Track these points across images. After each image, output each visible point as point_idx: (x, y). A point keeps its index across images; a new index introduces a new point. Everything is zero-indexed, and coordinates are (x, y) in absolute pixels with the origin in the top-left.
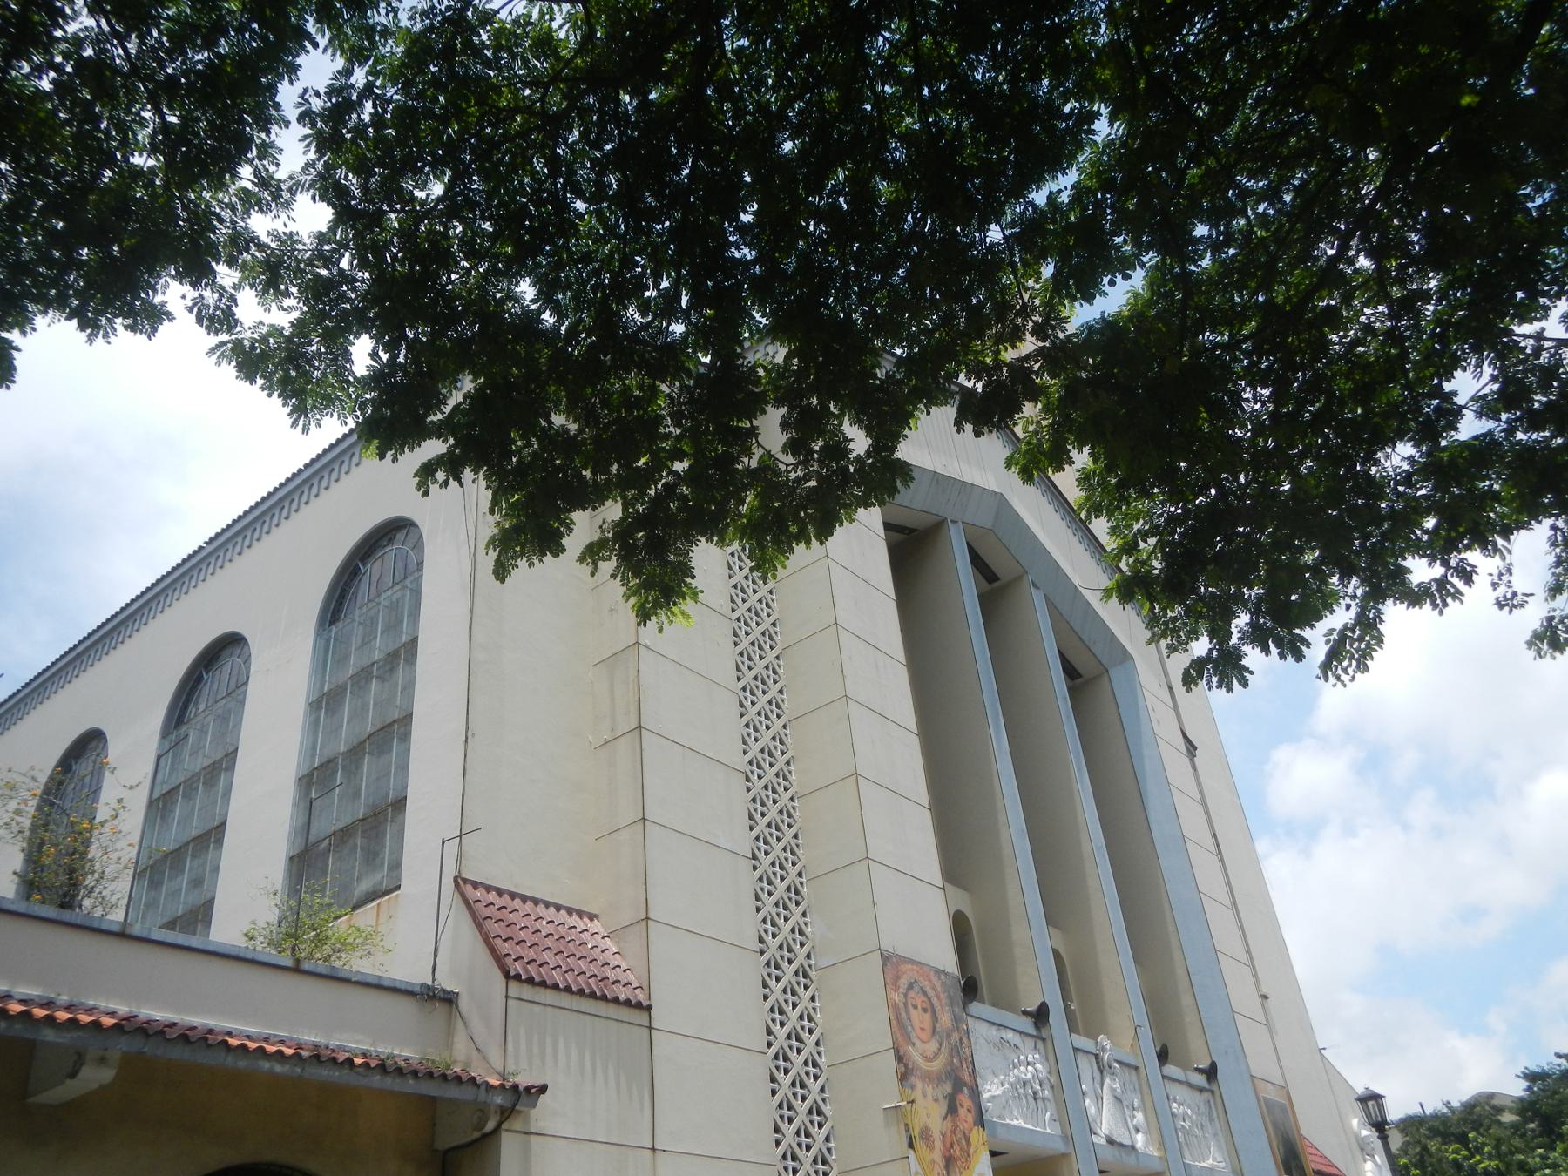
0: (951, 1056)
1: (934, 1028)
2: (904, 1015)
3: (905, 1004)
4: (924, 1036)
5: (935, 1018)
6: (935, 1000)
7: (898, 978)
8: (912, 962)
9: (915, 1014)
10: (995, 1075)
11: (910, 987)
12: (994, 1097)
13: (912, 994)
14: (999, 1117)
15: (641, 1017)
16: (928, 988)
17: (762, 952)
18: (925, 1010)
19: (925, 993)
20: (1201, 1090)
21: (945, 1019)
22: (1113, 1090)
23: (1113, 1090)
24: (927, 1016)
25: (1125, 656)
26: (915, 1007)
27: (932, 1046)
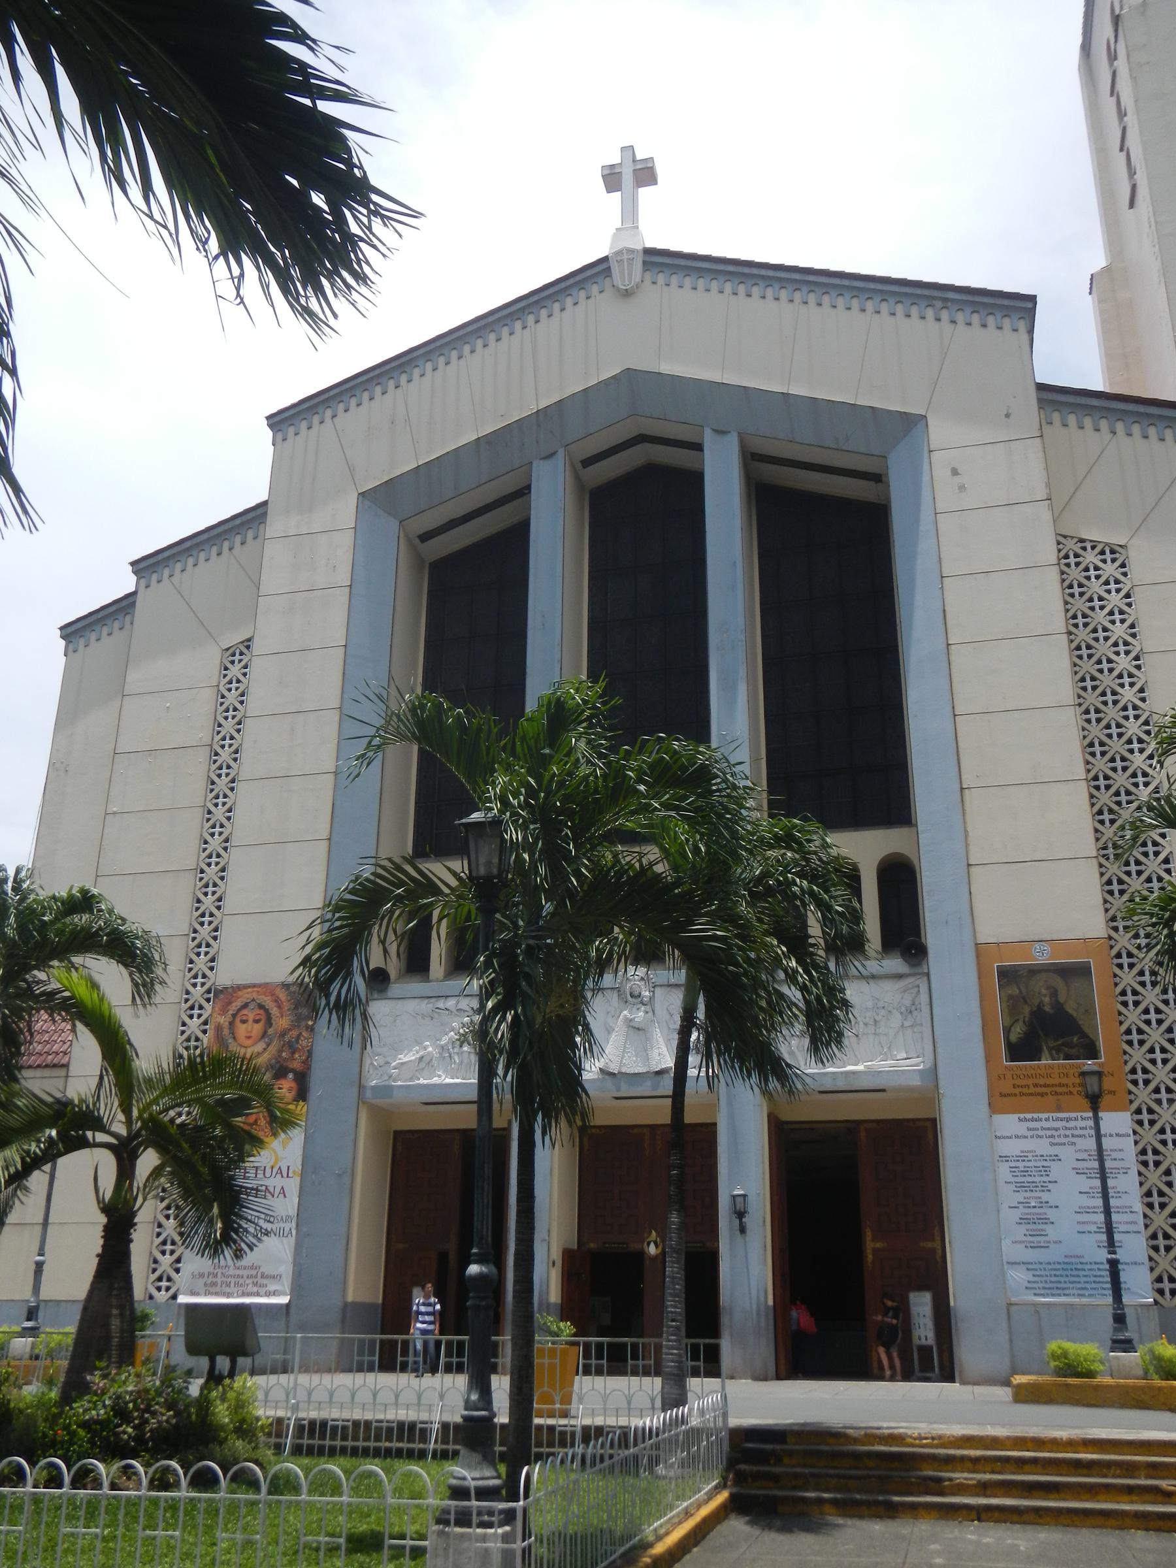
0: (280, 1051)
1: (265, 1033)
2: (226, 1031)
3: (231, 1024)
4: (248, 1042)
5: (269, 1022)
6: (274, 1011)
7: (230, 1003)
8: (254, 986)
9: (241, 1029)
10: (419, 1043)
11: (245, 1006)
12: (402, 1064)
13: (245, 1012)
14: (411, 1079)
15: (63, 1072)
16: (268, 1002)
17: (187, 1000)
18: (257, 1021)
19: (261, 1006)
20: (900, 976)
21: (282, 1022)
22: (629, 1022)
23: (629, 1022)
24: (258, 1028)
25: (909, 424)
26: (244, 1022)
27: (260, 1047)
